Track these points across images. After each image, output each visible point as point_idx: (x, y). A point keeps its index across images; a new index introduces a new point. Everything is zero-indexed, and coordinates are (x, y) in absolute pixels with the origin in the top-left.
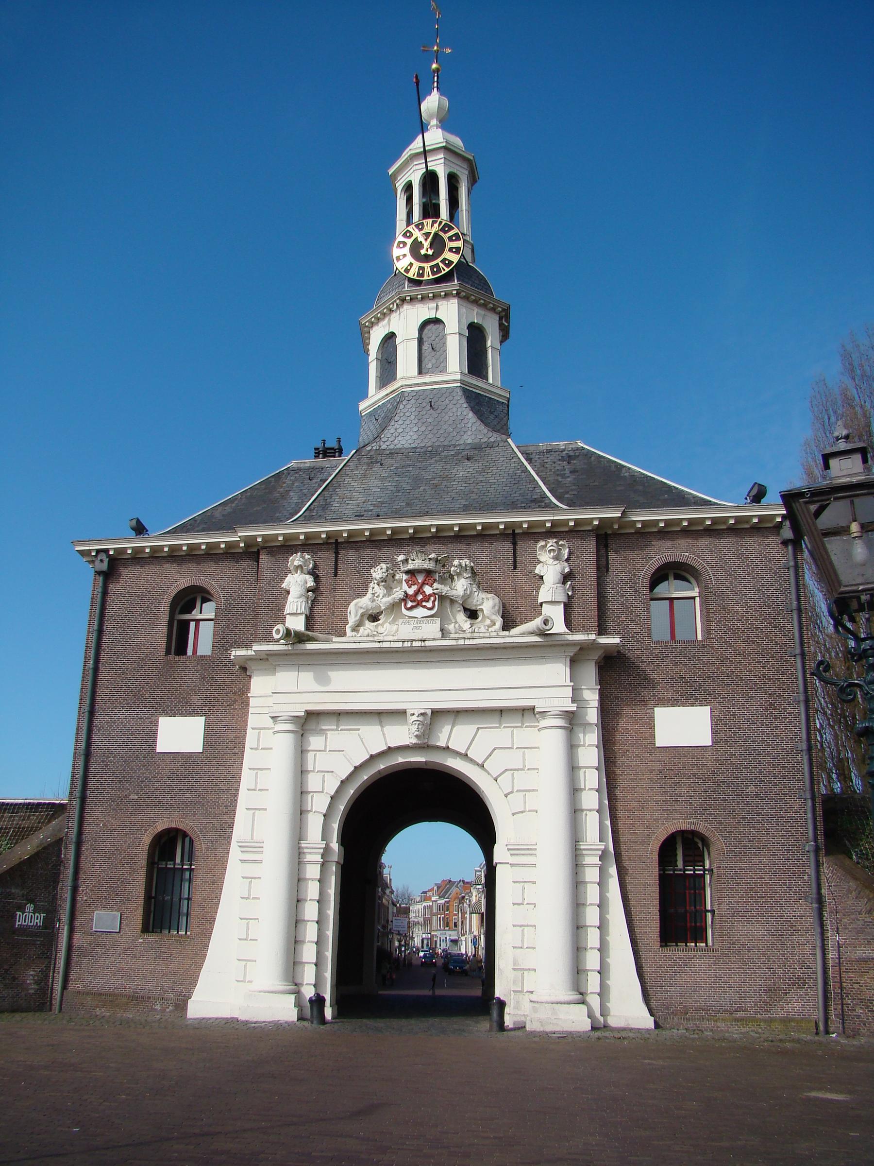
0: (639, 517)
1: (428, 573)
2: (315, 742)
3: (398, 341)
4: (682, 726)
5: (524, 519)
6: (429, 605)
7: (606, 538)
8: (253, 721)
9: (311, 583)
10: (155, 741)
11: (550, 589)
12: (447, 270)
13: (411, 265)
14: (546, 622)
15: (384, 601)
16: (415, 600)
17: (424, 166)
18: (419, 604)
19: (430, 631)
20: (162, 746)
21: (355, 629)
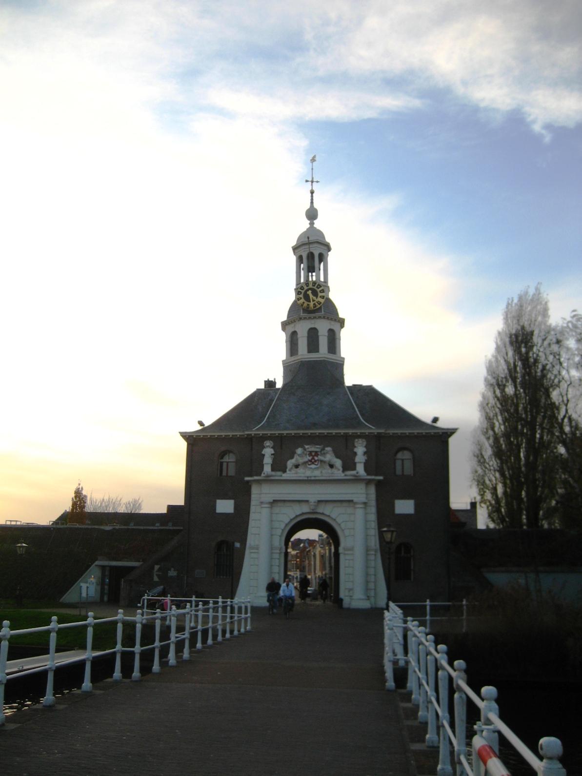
0: (391, 431)
1: (316, 452)
2: (276, 509)
3: (299, 336)
4: (405, 507)
5: (350, 431)
6: (316, 463)
7: (379, 437)
8: (253, 503)
9: (273, 452)
10: (215, 509)
12: (319, 306)
13: (304, 303)
14: (357, 473)
15: (301, 461)
16: (312, 462)
17: (308, 249)
18: (313, 463)
21: (290, 470)
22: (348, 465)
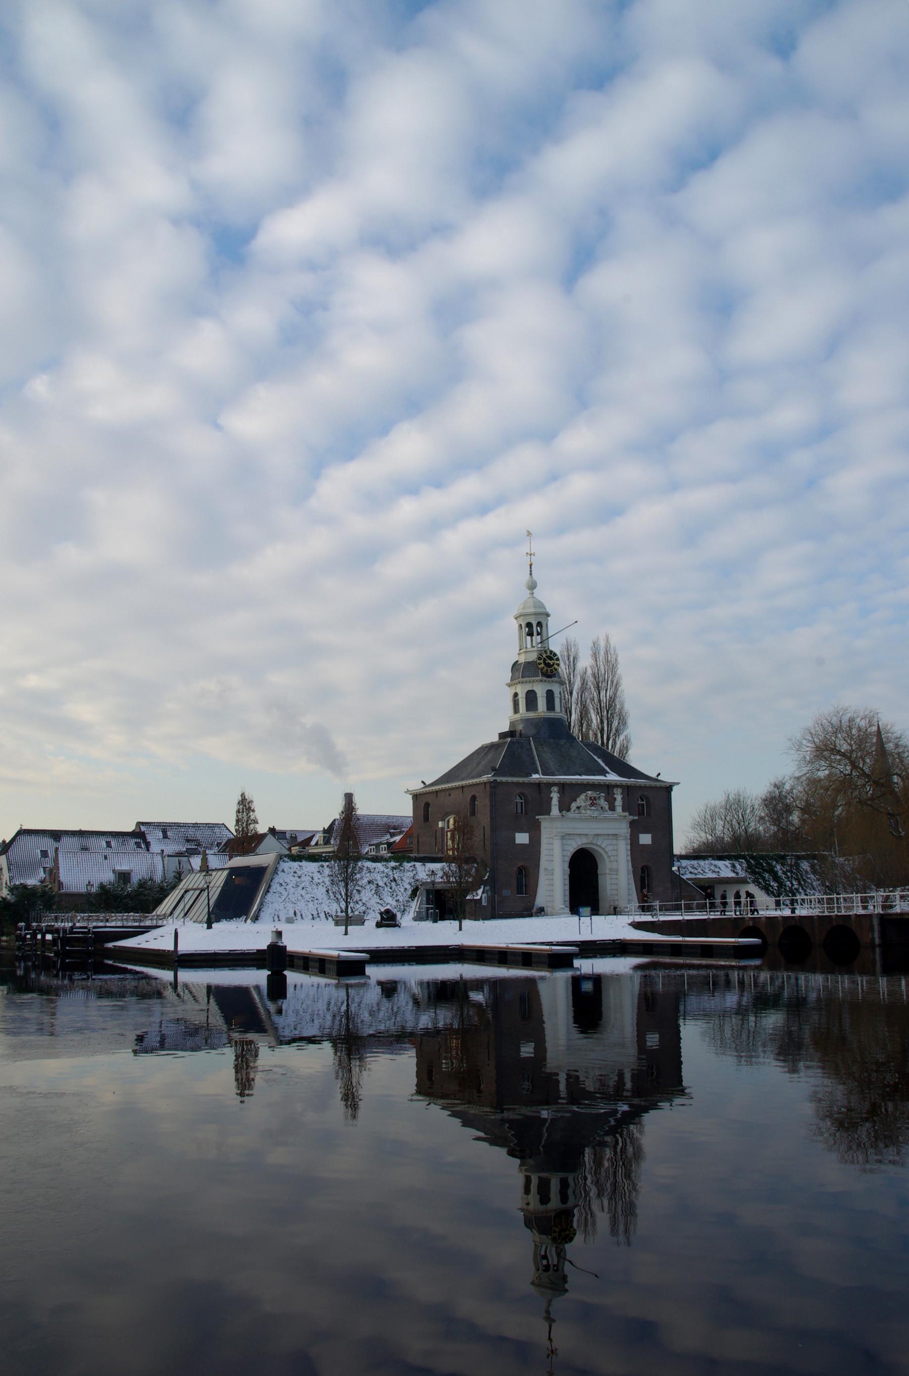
11: (619, 802)
16: (592, 805)
19: (596, 814)
20: (517, 842)
22: (612, 808)
